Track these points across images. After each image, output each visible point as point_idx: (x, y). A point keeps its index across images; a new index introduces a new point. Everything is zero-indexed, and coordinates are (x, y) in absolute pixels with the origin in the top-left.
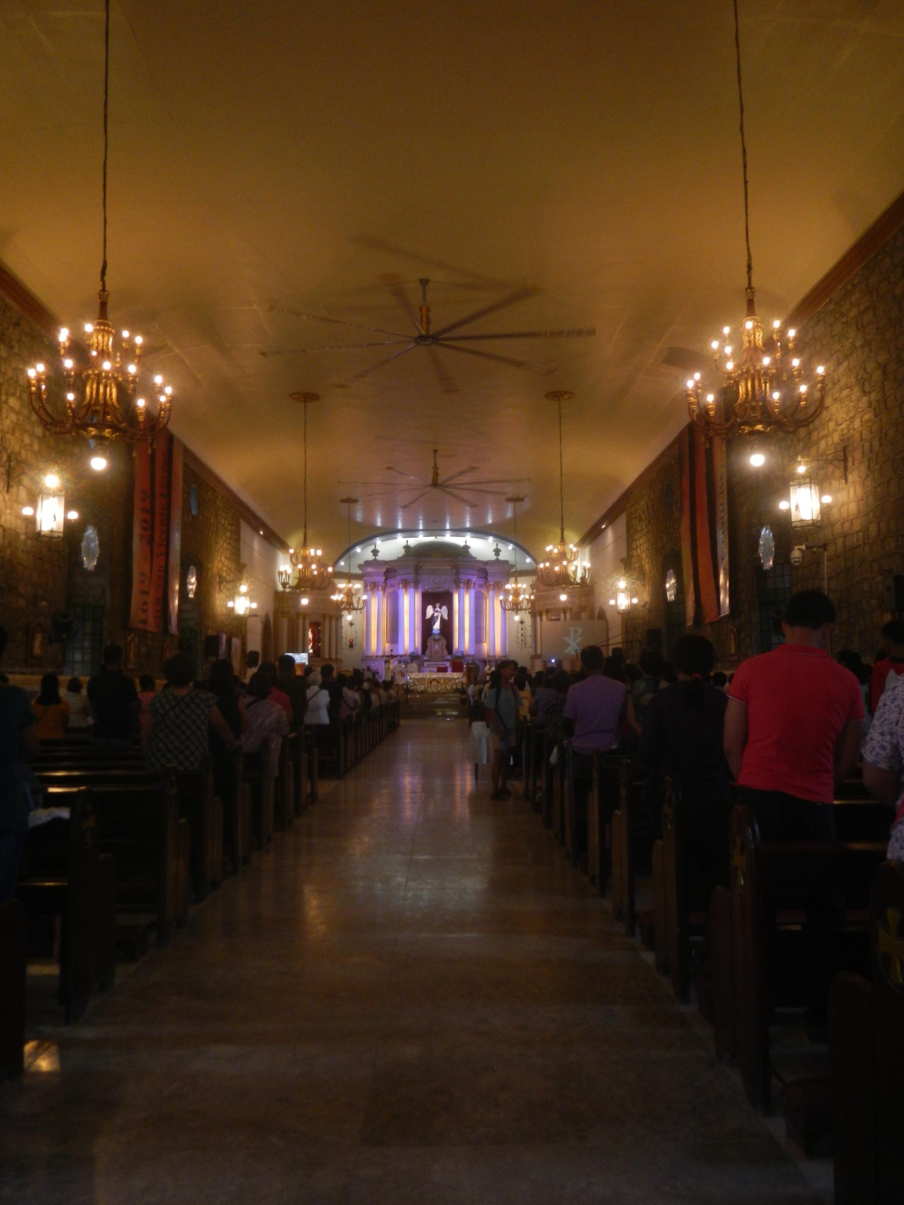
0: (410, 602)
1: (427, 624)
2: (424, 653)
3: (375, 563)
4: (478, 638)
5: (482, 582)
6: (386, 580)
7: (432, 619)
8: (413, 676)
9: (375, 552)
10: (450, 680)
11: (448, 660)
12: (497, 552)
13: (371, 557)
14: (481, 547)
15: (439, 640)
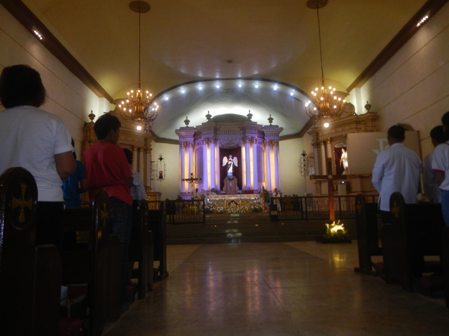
0: (211, 154)
1: (223, 170)
2: (221, 189)
5: (260, 140)
6: (194, 140)
7: (227, 166)
9: (187, 122)
10: (247, 201)
12: (271, 120)
13: (184, 125)
15: (232, 179)
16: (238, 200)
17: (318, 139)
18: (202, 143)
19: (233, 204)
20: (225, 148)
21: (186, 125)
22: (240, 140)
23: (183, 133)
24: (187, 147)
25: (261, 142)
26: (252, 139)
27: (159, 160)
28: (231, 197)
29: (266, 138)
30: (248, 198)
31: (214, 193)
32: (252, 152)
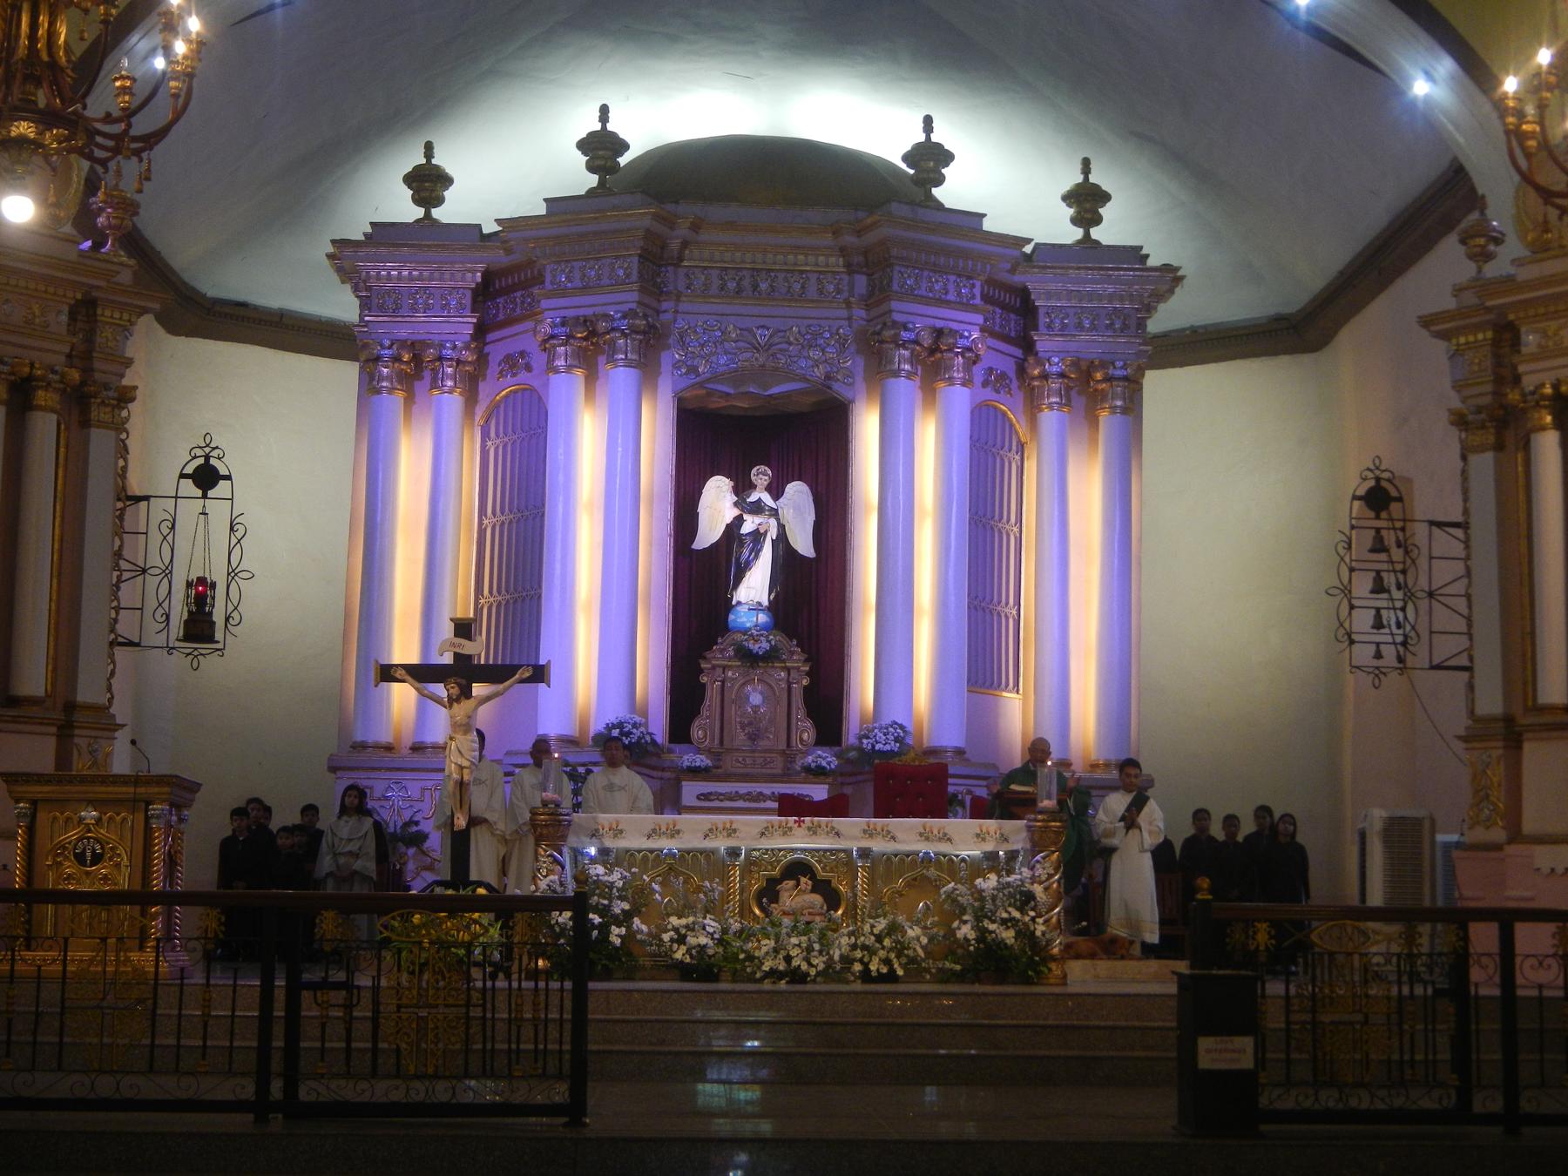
0: (607, 448)
2: (680, 727)
3: (427, 237)
4: (983, 649)
6: (481, 331)
7: (730, 554)
8: (626, 827)
9: (428, 183)
10: (920, 873)
11: (817, 773)
12: (1087, 202)
13: (402, 208)
14: (1004, 174)
15: (771, 656)
16: (846, 862)
17: (1506, 376)
18: (538, 360)
19: (797, 898)
20: (717, 403)
21: (420, 212)
22: (842, 344)
23: (392, 271)
24: (421, 387)
25: (1002, 376)
26: (933, 351)
27: (188, 487)
28: (787, 831)
29: (1043, 343)
30: (923, 847)
31: (626, 776)
32: (928, 438)
